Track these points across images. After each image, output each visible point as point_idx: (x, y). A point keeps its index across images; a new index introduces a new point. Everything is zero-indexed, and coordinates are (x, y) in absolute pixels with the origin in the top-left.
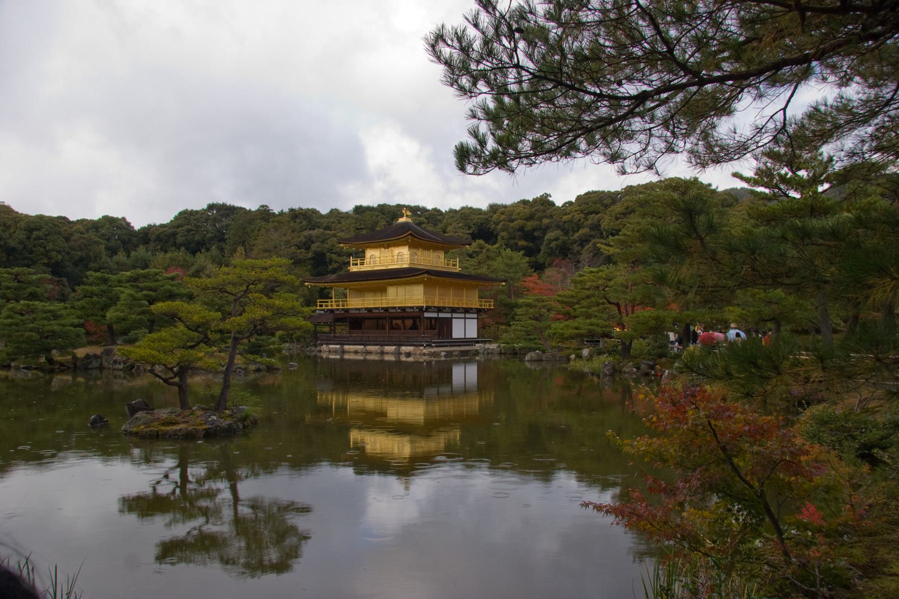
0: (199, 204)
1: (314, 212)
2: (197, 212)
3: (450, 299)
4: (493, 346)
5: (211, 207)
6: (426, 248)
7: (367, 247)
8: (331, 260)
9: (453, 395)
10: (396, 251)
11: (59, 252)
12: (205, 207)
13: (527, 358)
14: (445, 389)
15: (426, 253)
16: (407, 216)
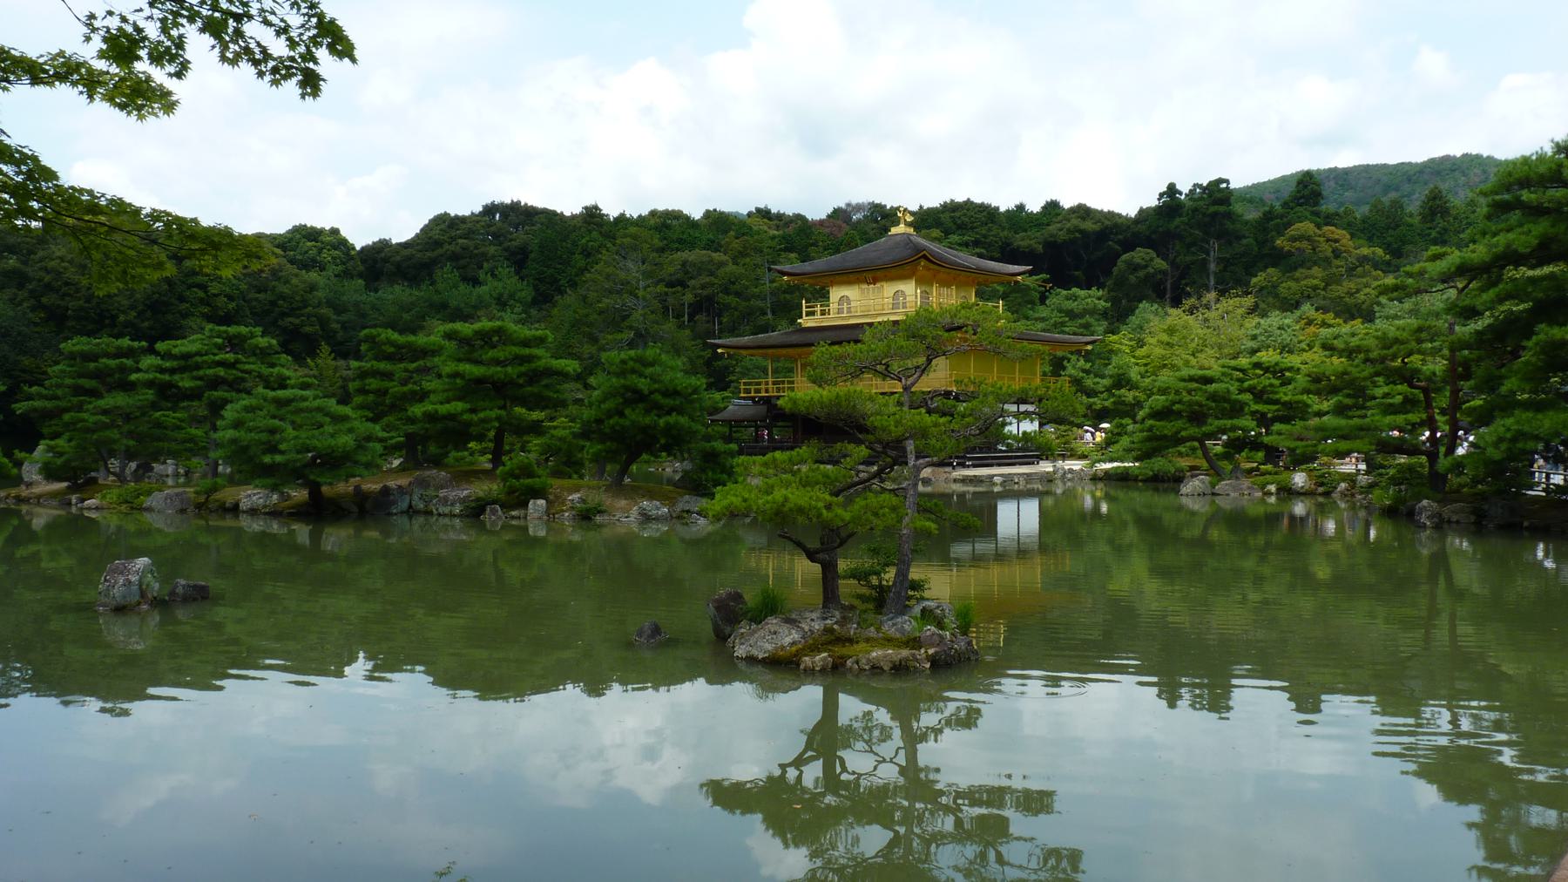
0: (466, 205)
1: (676, 216)
2: (463, 220)
3: (995, 377)
4: (1076, 465)
5: (490, 210)
6: (945, 284)
7: (832, 284)
8: (727, 307)
9: (1000, 557)
10: (889, 289)
11: (230, 298)
12: (478, 209)
13: (1186, 488)
14: (982, 547)
15: (945, 291)
16: (908, 224)
